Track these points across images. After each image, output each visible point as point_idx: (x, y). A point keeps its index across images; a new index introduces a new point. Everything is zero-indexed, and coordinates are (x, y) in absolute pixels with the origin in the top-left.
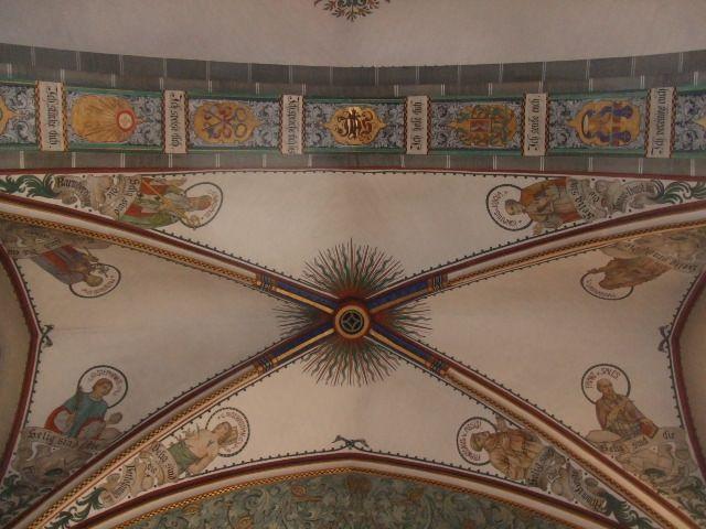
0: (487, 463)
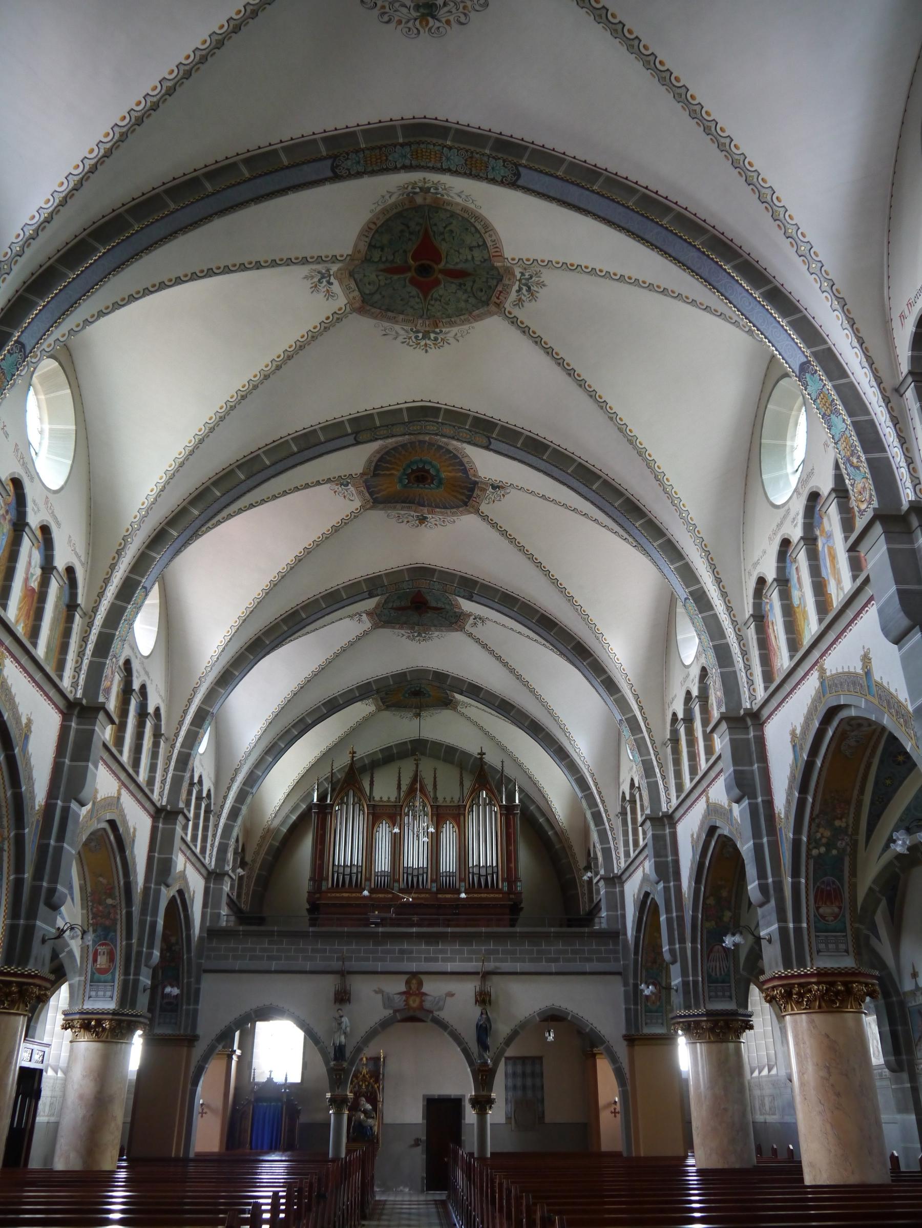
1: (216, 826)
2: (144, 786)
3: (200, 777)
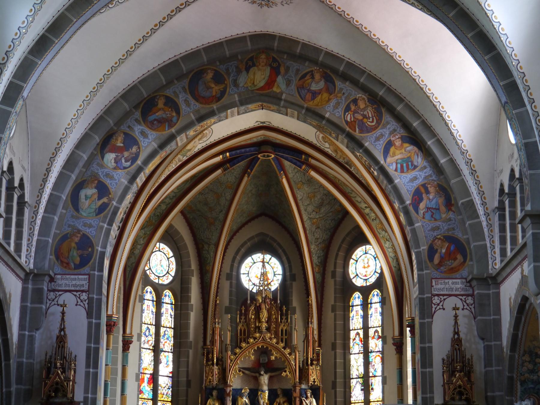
1: (32, 223)
2: (13, 253)
3: (22, 180)
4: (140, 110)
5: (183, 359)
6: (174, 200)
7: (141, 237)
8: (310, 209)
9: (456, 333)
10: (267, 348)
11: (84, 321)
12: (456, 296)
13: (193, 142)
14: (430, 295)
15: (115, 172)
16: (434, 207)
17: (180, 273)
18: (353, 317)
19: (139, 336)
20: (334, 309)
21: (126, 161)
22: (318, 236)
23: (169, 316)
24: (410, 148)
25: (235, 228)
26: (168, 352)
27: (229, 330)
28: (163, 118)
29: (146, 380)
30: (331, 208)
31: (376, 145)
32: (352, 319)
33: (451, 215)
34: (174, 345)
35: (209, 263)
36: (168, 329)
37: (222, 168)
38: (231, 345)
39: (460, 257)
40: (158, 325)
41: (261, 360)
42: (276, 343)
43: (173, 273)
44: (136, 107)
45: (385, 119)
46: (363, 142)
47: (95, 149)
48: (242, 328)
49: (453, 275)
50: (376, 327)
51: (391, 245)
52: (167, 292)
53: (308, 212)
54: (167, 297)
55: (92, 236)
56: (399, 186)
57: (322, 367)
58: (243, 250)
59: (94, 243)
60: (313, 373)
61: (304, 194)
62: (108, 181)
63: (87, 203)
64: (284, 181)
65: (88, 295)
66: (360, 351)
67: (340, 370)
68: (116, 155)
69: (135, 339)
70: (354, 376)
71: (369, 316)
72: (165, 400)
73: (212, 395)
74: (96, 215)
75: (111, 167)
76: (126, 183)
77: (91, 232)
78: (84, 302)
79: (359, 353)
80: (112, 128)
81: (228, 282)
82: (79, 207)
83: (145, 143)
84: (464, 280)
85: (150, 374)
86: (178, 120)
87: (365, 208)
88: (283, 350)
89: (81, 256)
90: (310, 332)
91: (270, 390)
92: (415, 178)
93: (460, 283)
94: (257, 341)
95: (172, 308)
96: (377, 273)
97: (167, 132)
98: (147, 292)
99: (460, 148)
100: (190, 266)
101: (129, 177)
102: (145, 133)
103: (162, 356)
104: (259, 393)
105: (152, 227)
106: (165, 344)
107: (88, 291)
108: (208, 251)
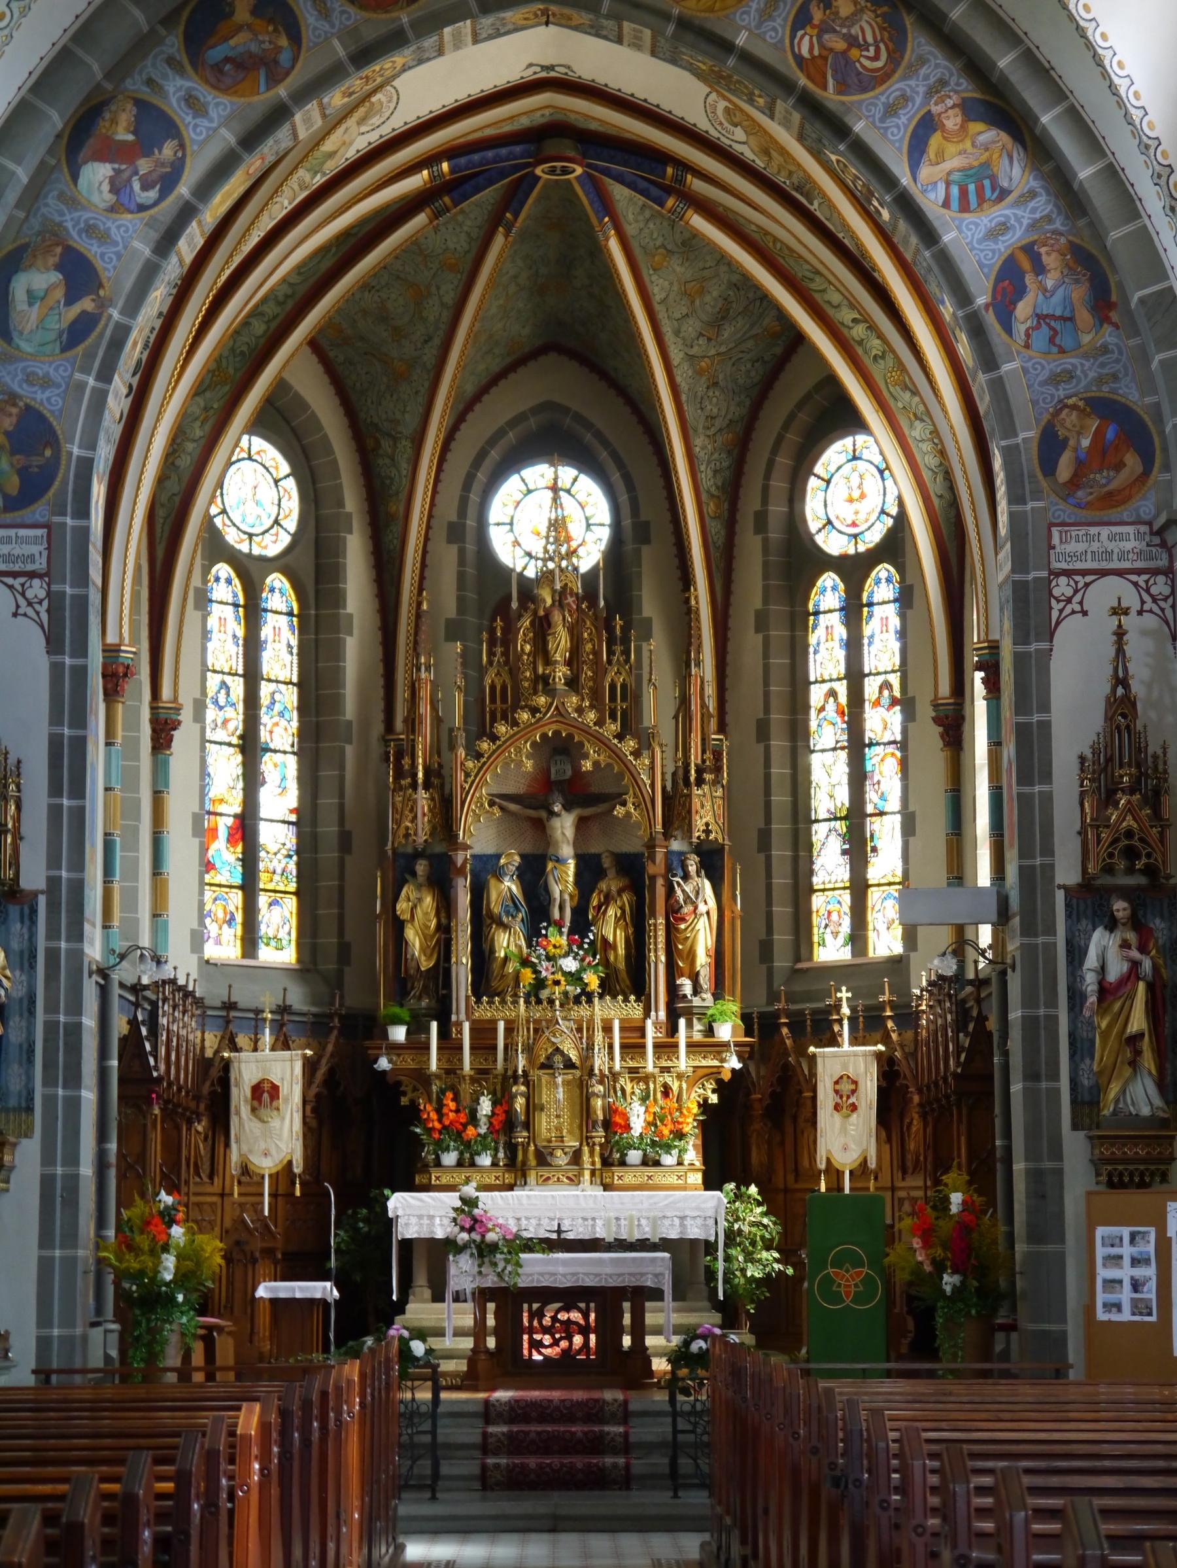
0: (744, 143)
4: (181, 28)
5: (327, 773)
6: (290, 305)
7: (197, 419)
8: (691, 328)
9: (1121, 680)
10: (570, 736)
11: (42, 662)
12: (1120, 573)
13: (340, 131)
14: (1045, 574)
15: (114, 221)
16: (1058, 313)
17: (312, 523)
18: (818, 644)
19: (200, 708)
20: (762, 622)
21: (145, 187)
22: (715, 411)
23: (284, 649)
24: (989, 135)
25: (470, 389)
26: (285, 752)
27: (459, 687)
28: (251, 55)
29: (223, 833)
30: (752, 326)
31: (887, 129)
32: (816, 652)
33: (1108, 335)
34: (302, 733)
35: (397, 493)
36: (282, 687)
37: (428, 210)
38: (465, 730)
39: (1132, 461)
40: (252, 675)
41: (553, 771)
42: (595, 724)
43: (291, 524)
44: (168, 21)
45: (913, 51)
46: (849, 120)
47: (51, 151)
48: (496, 680)
49: (1113, 514)
50: (886, 673)
51: (927, 432)
52: (277, 579)
53: (684, 339)
54: (277, 594)
55: (52, 412)
56: (954, 252)
57: (728, 790)
58: (494, 455)
59: (59, 432)
60: (703, 806)
61: (671, 284)
62: (95, 249)
63: (34, 313)
64: (614, 246)
65: (49, 585)
66: (837, 742)
67: (780, 799)
68: (114, 169)
69: (186, 716)
70: (822, 815)
71: (866, 641)
72: (278, 888)
73: (414, 874)
74: (64, 350)
75: (102, 205)
76: (147, 252)
77: (49, 399)
78: (37, 607)
79: (834, 749)
80: (98, 86)
81: (454, 549)
82: (12, 327)
83: (198, 130)
84: (1144, 529)
85: (236, 816)
86: (295, 60)
87: (851, 325)
88: (616, 741)
89: (23, 472)
90: (694, 690)
91: (579, 857)
92: (1003, 228)
93: (1132, 537)
94: (540, 719)
95: (292, 627)
96: (888, 515)
97: (264, 98)
98: (217, 579)
99: (1136, 132)
100: (341, 504)
101: (154, 235)
102: (198, 100)
103: (268, 763)
104: (550, 865)
105: (227, 388)
106: (276, 729)
107: (47, 574)
108: (393, 459)
